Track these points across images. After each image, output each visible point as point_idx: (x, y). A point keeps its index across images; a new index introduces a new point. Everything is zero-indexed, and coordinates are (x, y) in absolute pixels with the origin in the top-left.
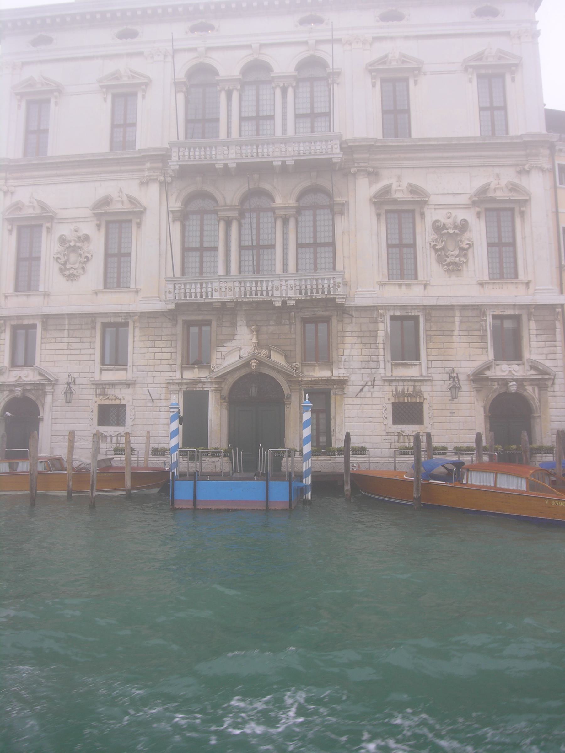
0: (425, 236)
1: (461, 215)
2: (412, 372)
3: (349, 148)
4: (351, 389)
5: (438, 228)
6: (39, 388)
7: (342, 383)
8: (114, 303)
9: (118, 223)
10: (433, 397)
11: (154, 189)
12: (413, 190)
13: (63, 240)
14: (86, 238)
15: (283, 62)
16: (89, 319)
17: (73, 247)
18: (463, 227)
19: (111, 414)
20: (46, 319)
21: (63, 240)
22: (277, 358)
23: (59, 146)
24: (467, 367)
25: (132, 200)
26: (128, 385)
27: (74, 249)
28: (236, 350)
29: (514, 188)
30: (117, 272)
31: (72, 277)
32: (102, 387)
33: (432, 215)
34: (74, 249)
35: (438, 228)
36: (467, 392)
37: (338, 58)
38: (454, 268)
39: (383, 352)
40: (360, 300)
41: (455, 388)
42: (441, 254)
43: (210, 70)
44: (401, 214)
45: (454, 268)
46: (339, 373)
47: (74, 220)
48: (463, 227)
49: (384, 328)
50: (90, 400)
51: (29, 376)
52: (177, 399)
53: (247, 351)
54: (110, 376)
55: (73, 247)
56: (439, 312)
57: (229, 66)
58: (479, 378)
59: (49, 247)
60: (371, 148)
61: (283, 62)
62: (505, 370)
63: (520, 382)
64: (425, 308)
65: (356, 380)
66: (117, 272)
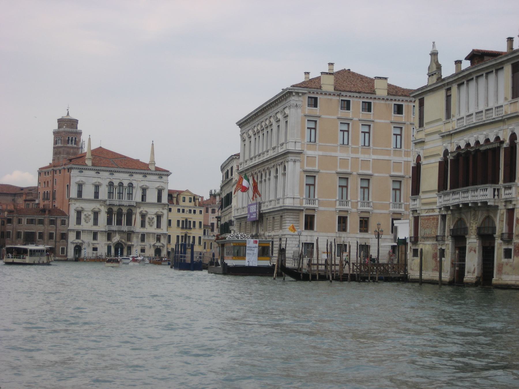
0: (147, 220)
1: (153, 216)
2: (143, 244)
3: (136, 203)
4: (134, 246)
5: (149, 218)
6: (82, 244)
7: (133, 245)
8: (95, 228)
9: (96, 214)
10: (147, 248)
11: (103, 207)
12: (146, 211)
13: (85, 215)
14: (90, 215)
15: (126, 184)
16: (91, 231)
17: (87, 217)
18: (153, 218)
19: (95, 249)
20: (83, 230)
21: (85, 215)
22: (123, 241)
23: (84, 196)
24: (152, 243)
25: (99, 209)
26: (98, 244)
27: (87, 217)
28: (116, 238)
29: (162, 212)
30: (96, 223)
31: (87, 222)
32: (93, 244)
33: (149, 216)
34: (87, 217)
35: (149, 218)
36: (152, 248)
37: (135, 184)
38: (151, 226)
39: (139, 240)
40: (137, 231)
41: (150, 247)
42: (149, 223)
43: (113, 183)
44: (143, 216)
45: (151, 226)
46: (133, 243)
47: (86, 211)
48: (153, 218)
49: (140, 236)
50: (92, 246)
51: (79, 241)
52: (106, 247)
53: (118, 239)
54: (95, 242)
55: (87, 217)
56: (148, 234)
57: (116, 183)
58: (154, 245)
59: (83, 216)
60: (139, 203)
61: (126, 184)
62: (158, 244)
63: (160, 246)
64: (147, 233)
65: (135, 245)
66: (96, 223)
